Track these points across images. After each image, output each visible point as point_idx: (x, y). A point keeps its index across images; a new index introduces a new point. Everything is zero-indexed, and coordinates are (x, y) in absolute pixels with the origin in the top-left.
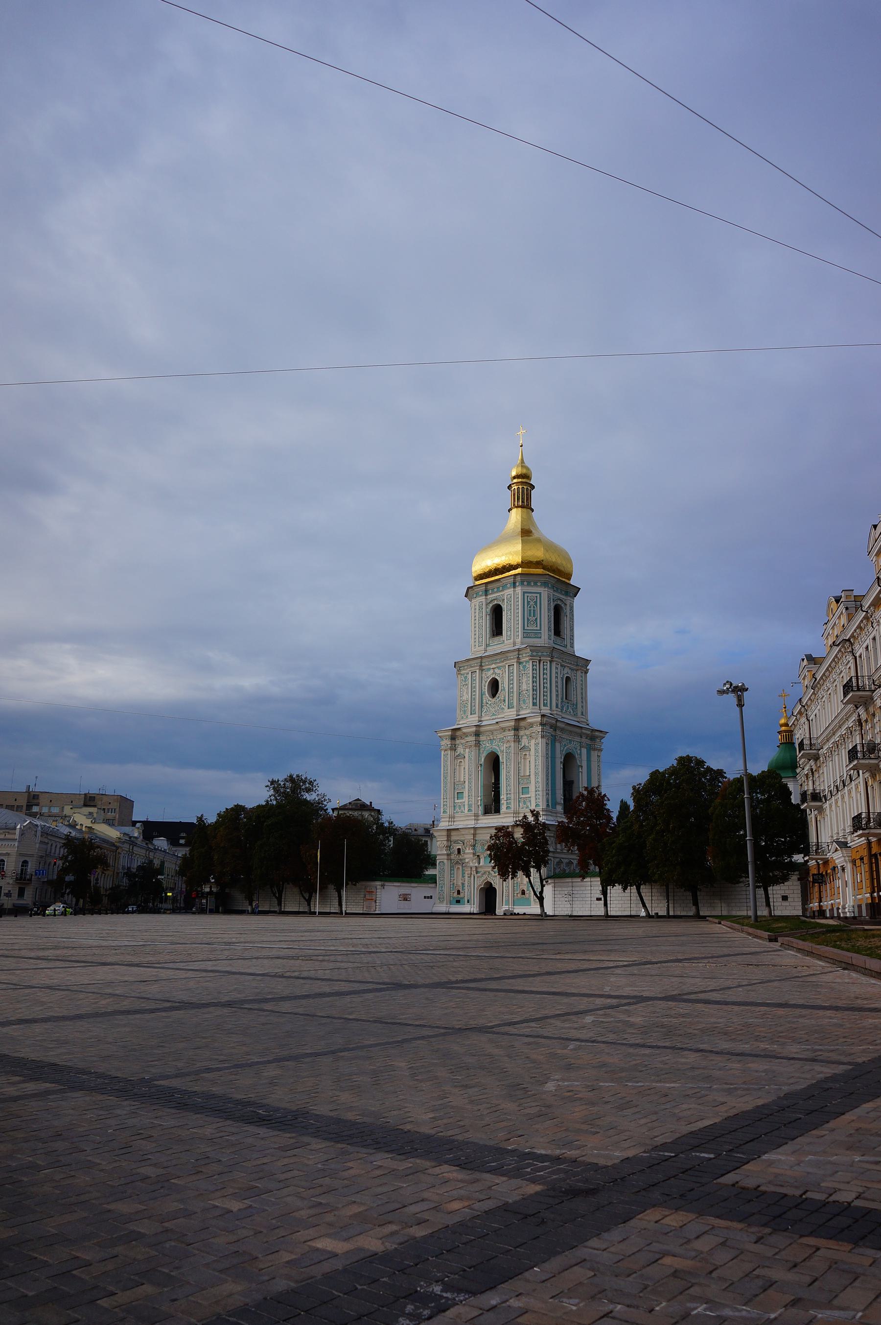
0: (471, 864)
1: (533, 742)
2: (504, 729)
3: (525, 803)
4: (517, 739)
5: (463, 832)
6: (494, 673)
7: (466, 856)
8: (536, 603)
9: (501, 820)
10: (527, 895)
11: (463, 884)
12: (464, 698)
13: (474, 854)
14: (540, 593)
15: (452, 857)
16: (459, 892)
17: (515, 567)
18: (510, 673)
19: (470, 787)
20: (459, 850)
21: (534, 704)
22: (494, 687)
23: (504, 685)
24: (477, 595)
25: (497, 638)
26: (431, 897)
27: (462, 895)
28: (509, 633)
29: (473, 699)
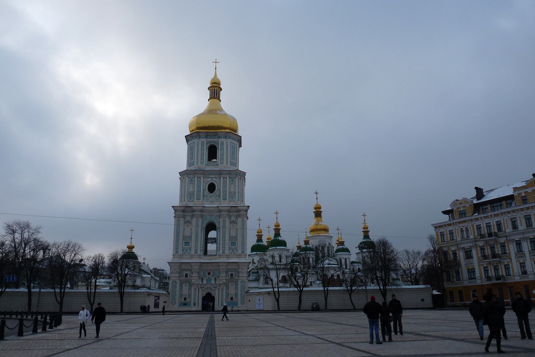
0: (196, 282)
2: (220, 211)
3: (233, 250)
6: (212, 180)
7: (191, 278)
11: (190, 295)
15: (181, 278)
16: (185, 299)
17: (225, 128)
18: (225, 182)
19: (196, 240)
20: (186, 275)
22: (212, 188)
24: (200, 137)
27: (188, 300)
28: (222, 161)
29: (199, 191)
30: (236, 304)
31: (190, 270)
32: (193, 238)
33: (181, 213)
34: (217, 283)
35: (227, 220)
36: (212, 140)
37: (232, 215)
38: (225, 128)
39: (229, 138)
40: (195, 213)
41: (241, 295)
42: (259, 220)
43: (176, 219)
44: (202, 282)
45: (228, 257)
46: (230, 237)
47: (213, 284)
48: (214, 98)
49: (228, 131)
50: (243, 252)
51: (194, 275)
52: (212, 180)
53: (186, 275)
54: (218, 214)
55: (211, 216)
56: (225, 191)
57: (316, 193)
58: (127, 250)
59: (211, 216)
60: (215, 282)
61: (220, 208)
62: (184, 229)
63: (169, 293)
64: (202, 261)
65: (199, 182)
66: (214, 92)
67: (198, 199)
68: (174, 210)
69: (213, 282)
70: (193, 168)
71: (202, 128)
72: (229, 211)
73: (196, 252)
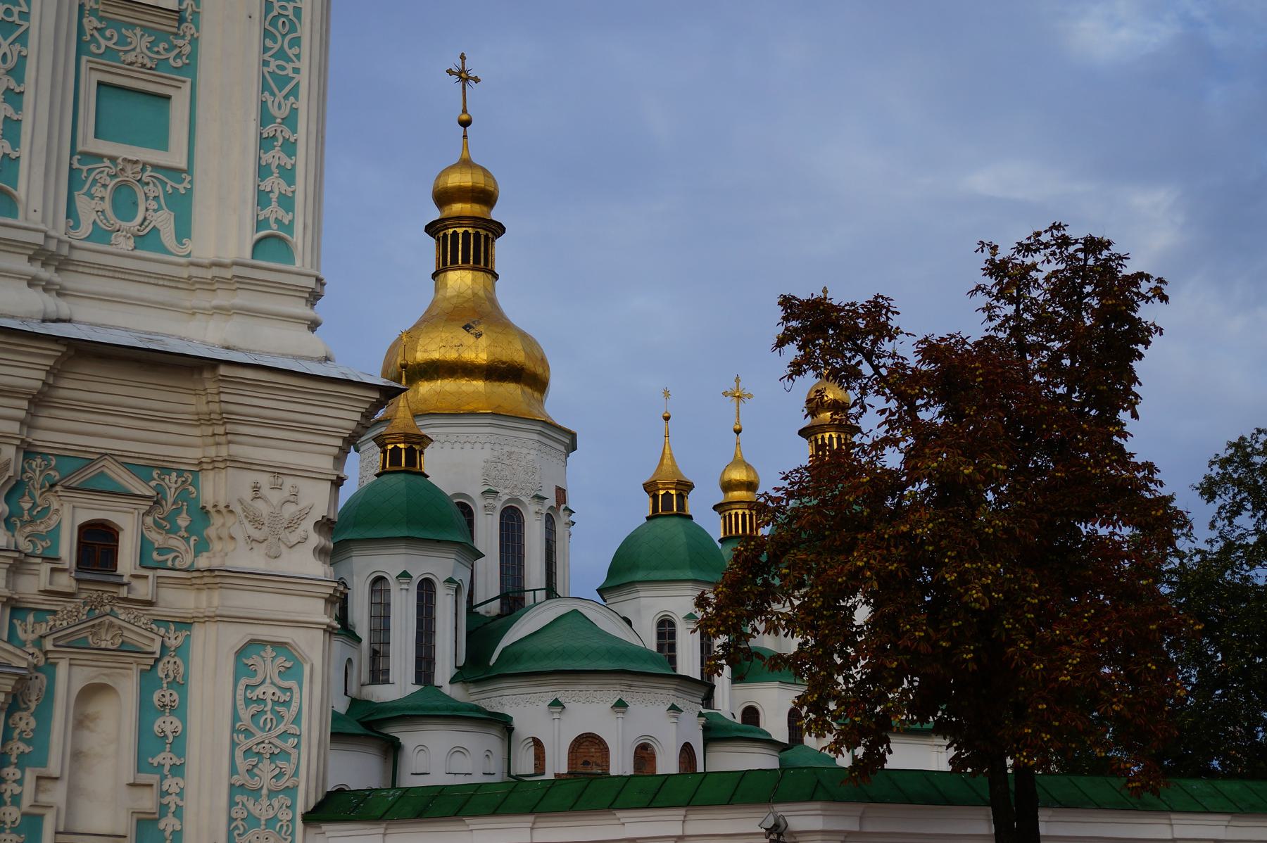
50: (271, 243)
57: (463, 77)
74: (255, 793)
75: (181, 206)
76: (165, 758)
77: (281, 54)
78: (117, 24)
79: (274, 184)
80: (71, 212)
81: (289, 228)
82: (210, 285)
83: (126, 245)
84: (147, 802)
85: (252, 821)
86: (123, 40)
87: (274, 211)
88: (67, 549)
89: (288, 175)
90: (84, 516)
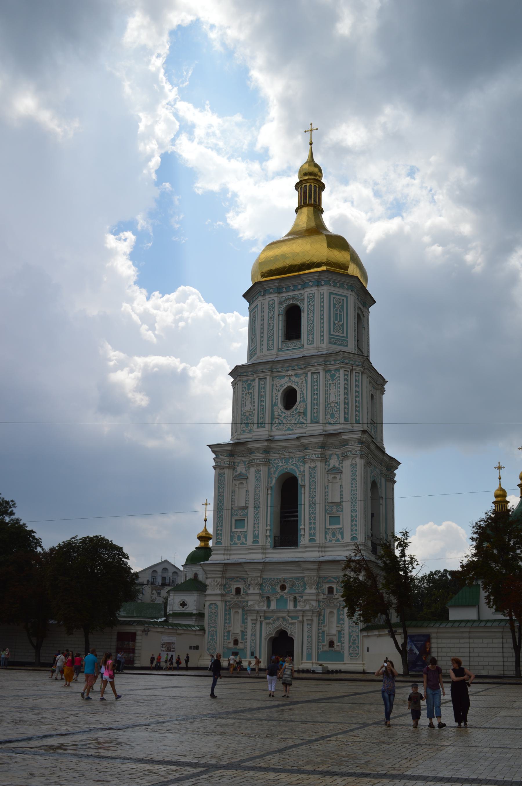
0: (257, 608)
1: (347, 463)
2: (305, 447)
3: (334, 535)
4: (325, 459)
5: (247, 567)
7: (247, 598)
8: (342, 306)
9: (300, 555)
10: (336, 648)
11: (244, 633)
12: (247, 408)
13: (261, 595)
14: (347, 297)
15: (228, 598)
16: (236, 642)
17: (319, 265)
19: (256, 516)
20: (238, 591)
21: (346, 419)
22: (290, 398)
23: (304, 394)
24: (266, 292)
25: (292, 344)
26: (197, 648)
27: (240, 646)
28: (311, 337)
29: (261, 409)
30: (339, 656)
31: (245, 580)
32: (251, 511)
33: (226, 460)
34: (298, 608)
35: (319, 465)
36: (290, 296)
37: (331, 456)
38: (319, 265)
39: (327, 283)
40: (254, 456)
41: (350, 636)
42: (499, 468)
43: (218, 470)
44: (269, 606)
45: (322, 547)
46: (328, 505)
47: (289, 611)
48: (305, 205)
49: (324, 268)
51: (251, 591)
52: (290, 380)
53: (238, 591)
54: (301, 454)
55: (287, 460)
56: (315, 404)
58: (198, 543)
59: (287, 460)
60: (295, 606)
61: (304, 441)
62: (233, 492)
63: (203, 629)
64: (267, 560)
65: (262, 388)
66: (305, 193)
67: (261, 425)
68: (214, 452)
69: (290, 606)
70: (253, 361)
71: (271, 273)
72: (323, 446)
73: (255, 541)
74: (353, 627)
75: (342, 533)
76: (342, 622)
77: (354, 505)
78: (331, 506)
79: (354, 527)
80: (326, 538)
81: (356, 534)
82: (346, 546)
83: (334, 542)
84: (339, 629)
85: (352, 631)
86: (332, 509)
87: (354, 532)
88: (326, 592)
89: (356, 525)
90: (328, 586)
